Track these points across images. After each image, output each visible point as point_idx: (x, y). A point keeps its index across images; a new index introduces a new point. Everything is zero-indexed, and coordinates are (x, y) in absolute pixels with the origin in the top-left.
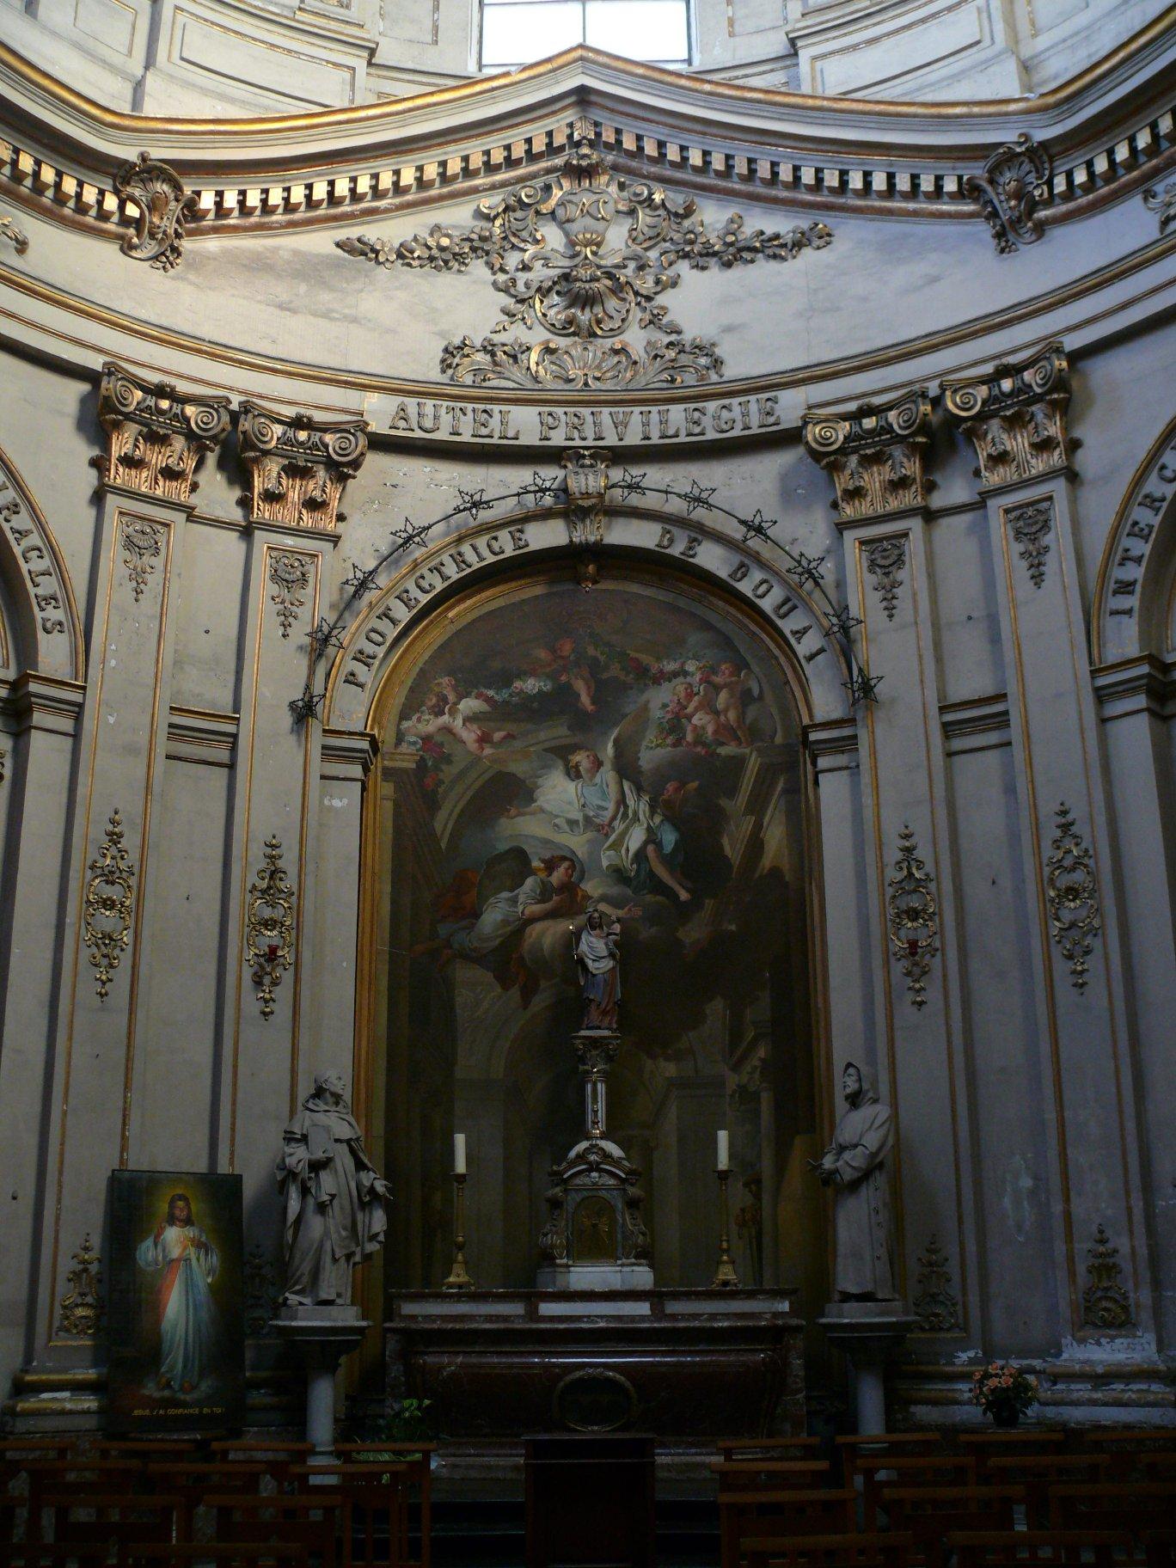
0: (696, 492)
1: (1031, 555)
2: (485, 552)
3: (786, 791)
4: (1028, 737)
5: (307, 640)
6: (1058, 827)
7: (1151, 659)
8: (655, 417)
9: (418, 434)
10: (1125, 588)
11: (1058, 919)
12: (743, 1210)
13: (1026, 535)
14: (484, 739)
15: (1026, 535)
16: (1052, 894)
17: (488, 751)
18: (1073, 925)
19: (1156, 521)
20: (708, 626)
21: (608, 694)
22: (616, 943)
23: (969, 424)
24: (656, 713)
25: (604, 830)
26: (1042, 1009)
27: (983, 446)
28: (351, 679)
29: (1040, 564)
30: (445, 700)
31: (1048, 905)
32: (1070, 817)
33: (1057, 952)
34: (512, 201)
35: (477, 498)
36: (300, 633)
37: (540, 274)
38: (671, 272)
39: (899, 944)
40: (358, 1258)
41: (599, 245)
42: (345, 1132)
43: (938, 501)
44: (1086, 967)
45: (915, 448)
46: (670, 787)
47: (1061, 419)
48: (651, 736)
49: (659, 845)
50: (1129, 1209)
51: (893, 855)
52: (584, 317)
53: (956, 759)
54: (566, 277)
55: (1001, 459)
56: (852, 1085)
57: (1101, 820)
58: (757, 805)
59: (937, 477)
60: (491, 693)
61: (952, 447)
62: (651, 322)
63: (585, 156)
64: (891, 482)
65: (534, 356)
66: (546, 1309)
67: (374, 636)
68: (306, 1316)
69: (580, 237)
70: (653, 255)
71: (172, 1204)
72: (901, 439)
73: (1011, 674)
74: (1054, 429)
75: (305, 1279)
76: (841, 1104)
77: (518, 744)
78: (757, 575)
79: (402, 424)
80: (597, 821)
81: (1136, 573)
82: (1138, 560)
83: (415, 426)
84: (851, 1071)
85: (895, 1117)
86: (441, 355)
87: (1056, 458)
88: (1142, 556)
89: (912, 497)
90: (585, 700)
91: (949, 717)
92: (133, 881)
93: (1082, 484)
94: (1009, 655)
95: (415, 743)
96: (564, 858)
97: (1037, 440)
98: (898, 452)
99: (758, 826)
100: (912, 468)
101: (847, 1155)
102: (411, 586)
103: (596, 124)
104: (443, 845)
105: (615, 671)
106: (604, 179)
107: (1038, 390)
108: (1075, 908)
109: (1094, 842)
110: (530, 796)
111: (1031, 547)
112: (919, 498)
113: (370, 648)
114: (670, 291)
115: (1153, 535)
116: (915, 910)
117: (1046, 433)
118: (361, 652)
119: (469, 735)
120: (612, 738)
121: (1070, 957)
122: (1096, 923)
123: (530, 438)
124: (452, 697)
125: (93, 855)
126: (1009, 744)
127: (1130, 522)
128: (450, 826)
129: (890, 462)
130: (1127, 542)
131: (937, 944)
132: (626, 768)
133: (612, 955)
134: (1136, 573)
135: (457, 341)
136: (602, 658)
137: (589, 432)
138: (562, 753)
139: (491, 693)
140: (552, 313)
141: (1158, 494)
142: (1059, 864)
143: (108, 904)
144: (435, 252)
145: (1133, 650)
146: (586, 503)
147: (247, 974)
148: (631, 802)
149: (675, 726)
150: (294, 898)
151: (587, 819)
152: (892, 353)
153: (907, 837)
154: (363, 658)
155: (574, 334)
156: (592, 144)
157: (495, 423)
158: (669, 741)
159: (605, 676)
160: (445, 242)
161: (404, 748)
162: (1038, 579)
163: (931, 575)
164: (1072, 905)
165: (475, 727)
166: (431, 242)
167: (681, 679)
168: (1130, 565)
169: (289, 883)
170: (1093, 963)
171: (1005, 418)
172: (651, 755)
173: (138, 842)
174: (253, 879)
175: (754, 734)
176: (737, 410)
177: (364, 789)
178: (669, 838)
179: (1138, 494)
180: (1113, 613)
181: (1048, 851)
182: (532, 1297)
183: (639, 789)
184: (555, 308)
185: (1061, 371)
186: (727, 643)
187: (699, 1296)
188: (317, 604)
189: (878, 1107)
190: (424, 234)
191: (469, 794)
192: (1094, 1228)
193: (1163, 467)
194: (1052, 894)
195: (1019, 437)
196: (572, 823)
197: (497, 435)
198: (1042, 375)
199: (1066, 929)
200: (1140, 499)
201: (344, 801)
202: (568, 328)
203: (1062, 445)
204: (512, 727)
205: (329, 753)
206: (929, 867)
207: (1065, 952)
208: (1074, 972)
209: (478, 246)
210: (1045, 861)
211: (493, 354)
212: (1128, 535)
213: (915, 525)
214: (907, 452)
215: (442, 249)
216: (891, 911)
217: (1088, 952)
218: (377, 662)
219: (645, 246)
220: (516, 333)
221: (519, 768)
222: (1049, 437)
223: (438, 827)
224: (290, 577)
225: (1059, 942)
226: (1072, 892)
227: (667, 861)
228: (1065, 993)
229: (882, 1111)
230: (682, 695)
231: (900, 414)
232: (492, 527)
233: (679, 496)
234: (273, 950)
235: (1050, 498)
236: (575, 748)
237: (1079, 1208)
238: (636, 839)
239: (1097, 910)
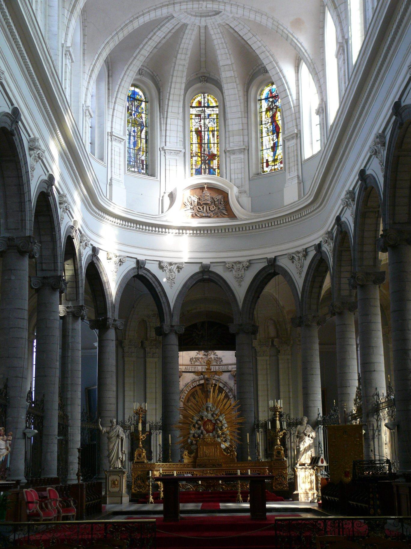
78: (226, 388)
157: (196, 368)
176: (224, 368)
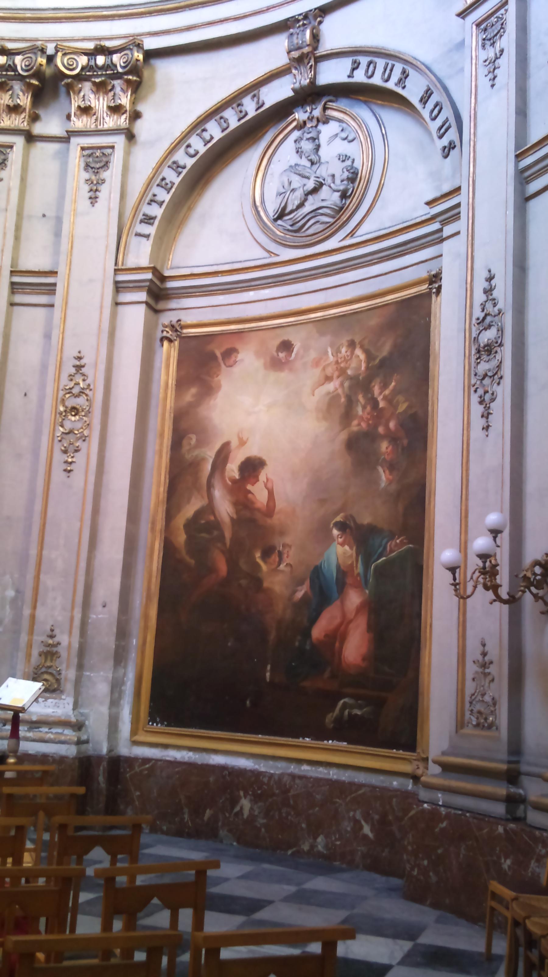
1: (92, 183)
4: (66, 303)
6: (74, 366)
7: (155, 270)
10: (148, 220)
11: (62, 426)
13: (92, 168)
15: (92, 168)
16: (62, 409)
18: (71, 432)
19: (177, 180)
23: (69, 80)
27: (76, 99)
29: (97, 190)
31: (58, 416)
32: (83, 362)
43: (38, 129)
44: (74, 460)
45: (29, 86)
47: (131, 95)
50: (72, 619)
53: (16, 308)
55: (86, 110)
57: (102, 367)
59: (41, 112)
61: (55, 94)
64: (8, 106)
72: (21, 78)
73: (63, 258)
74: (125, 100)
81: (157, 211)
82: (161, 204)
87: (122, 121)
88: (163, 202)
89: (21, 121)
91: (17, 279)
93: (135, 143)
94: (65, 246)
97: (112, 104)
98: (17, 86)
100: (25, 100)
107: (120, 70)
108: (75, 421)
109: (94, 381)
111: (93, 177)
112: (25, 124)
115: (173, 190)
117: (119, 102)
121: (65, 452)
122: (86, 433)
126: (52, 306)
127: (161, 177)
129: (10, 92)
130: (156, 190)
134: (157, 211)
141: (181, 163)
142: (69, 391)
145: (145, 262)
152: (28, 15)
162: (93, 200)
163: (23, 180)
164: (73, 418)
168: (154, 205)
170: (80, 458)
171: (94, 83)
179: (169, 160)
180: (138, 235)
181: (64, 381)
185: (137, 60)
192: (48, 628)
193: (189, 146)
194: (62, 409)
195: (101, 99)
198: (125, 60)
199: (66, 434)
200: (170, 163)
203: (128, 113)
207: (63, 448)
208: (66, 462)
210: (61, 387)
212: (158, 185)
213: (19, 141)
214: (23, 88)
217: (77, 451)
222: (120, 105)
225: (60, 441)
226: (75, 410)
228: (58, 474)
231: (24, 59)
235: (113, 147)
237: (41, 613)
239: (88, 425)
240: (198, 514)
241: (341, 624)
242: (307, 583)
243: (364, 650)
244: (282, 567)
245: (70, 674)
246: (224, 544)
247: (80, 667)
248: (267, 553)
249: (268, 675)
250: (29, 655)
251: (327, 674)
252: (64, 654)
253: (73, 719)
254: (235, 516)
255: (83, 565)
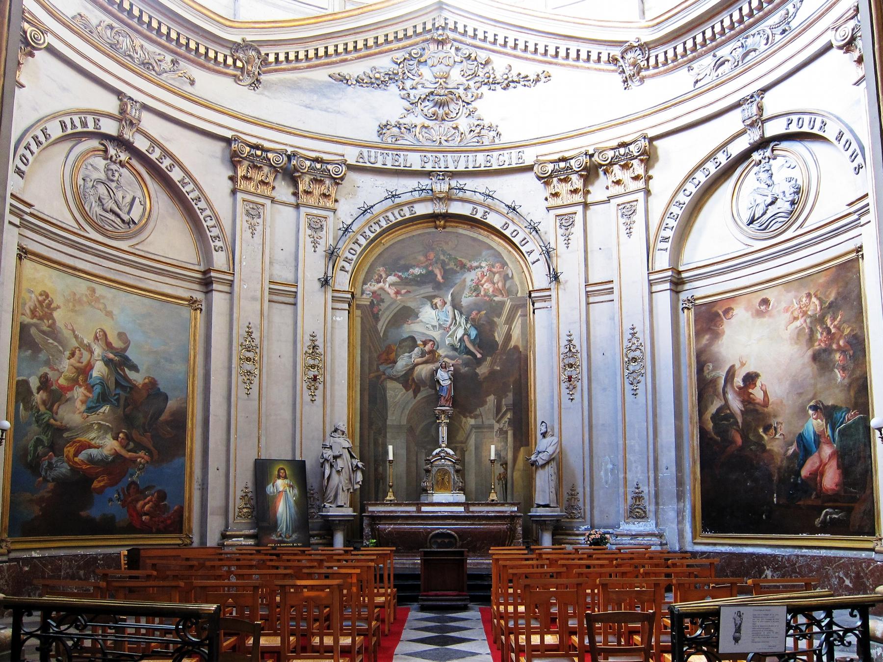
0: (487, 192)
2: (398, 216)
3: (521, 316)
5: (324, 253)
8: (471, 159)
9: (368, 165)
12: (500, 474)
14: (397, 293)
17: (399, 297)
18: (634, 372)
20: (491, 248)
21: (447, 274)
22: (451, 374)
24: (468, 283)
25: (447, 330)
26: (619, 403)
28: (343, 269)
30: (381, 276)
33: (626, 381)
34: (407, 56)
35: (394, 193)
36: (321, 249)
37: (421, 92)
38: (479, 91)
39: (563, 377)
40: (351, 491)
41: (446, 78)
42: (347, 445)
46: (474, 313)
48: (466, 292)
49: (469, 336)
51: (564, 342)
52: (441, 112)
54: (432, 93)
56: (544, 430)
58: (510, 320)
60: (400, 274)
62: (469, 115)
63: (440, 35)
65: (418, 129)
66: (424, 509)
67: (351, 251)
68: (333, 511)
69: (438, 74)
70: (471, 83)
71: (279, 471)
75: (332, 498)
76: (539, 436)
77: (411, 295)
79: (361, 160)
80: (444, 326)
83: (367, 161)
84: (543, 424)
85: (560, 442)
86: (377, 128)
90: (439, 277)
92: (258, 350)
95: (369, 294)
96: (431, 340)
99: (510, 329)
101: (540, 455)
102: (367, 230)
103: (446, 19)
104: (381, 335)
105: (452, 265)
106: (449, 45)
110: (417, 316)
113: (350, 256)
114: (479, 100)
116: (571, 364)
118: (346, 258)
119: (392, 291)
120: (451, 292)
121: (632, 384)
123: (417, 167)
124: (384, 276)
125: (241, 340)
128: (384, 327)
131: (580, 377)
132: (456, 306)
133: (450, 379)
135: (384, 123)
136: (447, 260)
137: (442, 165)
138: (430, 298)
139: (400, 274)
140: (425, 110)
143: (248, 359)
144: (373, 80)
146: (441, 196)
147: (305, 385)
148: (458, 318)
149: (476, 289)
150: (322, 356)
151: (440, 325)
153: (570, 336)
154: (346, 260)
155: (436, 119)
156: (443, 29)
157: (401, 160)
158: (474, 294)
159: (448, 267)
160: (377, 76)
161: (364, 296)
164: (634, 364)
165: (394, 288)
166: (371, 76)
167: (479, 269)
169: (320, 350)
172: (466, 300)
173: (259, 335)
174: (306, 349)
175: (509, 292)
177: (349, 313)
178: (473, 333)
182: (419, 505)
183: (461, 313)
184: (429, 107)
186: (498, 255)
187: (482, 504)
188: (327, 238)
189: (553, 438)
190: (368, 71)
191: (391, 316)
196: (434, 327)
197: (402, 165)
201: (342, 318)
202: (434, 117)
204: (409, 288)
205: (334, 299)
206: (578, 348)
209: (392, 77)
211: (399, 128)
215: (377, 79)
216: (562, 364)
218: (353, 262)
219: (468, 78)
220: (410, 120)
221: (412, 304)
223: (379, 327)
224: (316, 226)
227: (473, 342)
228: (629, 397)
229: (555, 439)
230: (480, 276)
232: (400, 205)
233: (480, 193)
234: (315, 377)
236: (434, 297)
238: (460, 333)
240: (719, 410)
241: (820, 466)
242: (795, 444)
243: (836, 480)
244: (777, 436)
245: (651, 508)
246: (739, 427)
247: (657, 504)
248: (767, 429)
249: (775, 499)
250: (626, 500)
251: (813, 497)
252: (646, 497)
253: (657, 532)
254: (743, 409)
255: (651, 447)
